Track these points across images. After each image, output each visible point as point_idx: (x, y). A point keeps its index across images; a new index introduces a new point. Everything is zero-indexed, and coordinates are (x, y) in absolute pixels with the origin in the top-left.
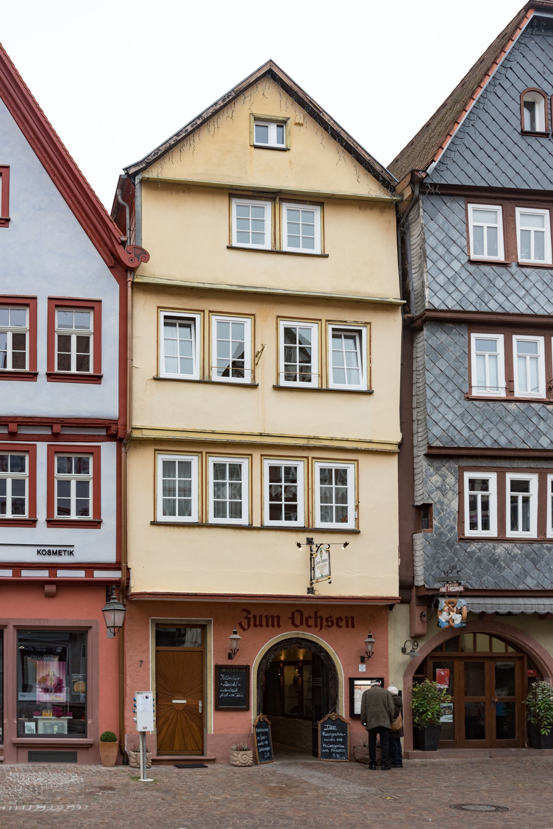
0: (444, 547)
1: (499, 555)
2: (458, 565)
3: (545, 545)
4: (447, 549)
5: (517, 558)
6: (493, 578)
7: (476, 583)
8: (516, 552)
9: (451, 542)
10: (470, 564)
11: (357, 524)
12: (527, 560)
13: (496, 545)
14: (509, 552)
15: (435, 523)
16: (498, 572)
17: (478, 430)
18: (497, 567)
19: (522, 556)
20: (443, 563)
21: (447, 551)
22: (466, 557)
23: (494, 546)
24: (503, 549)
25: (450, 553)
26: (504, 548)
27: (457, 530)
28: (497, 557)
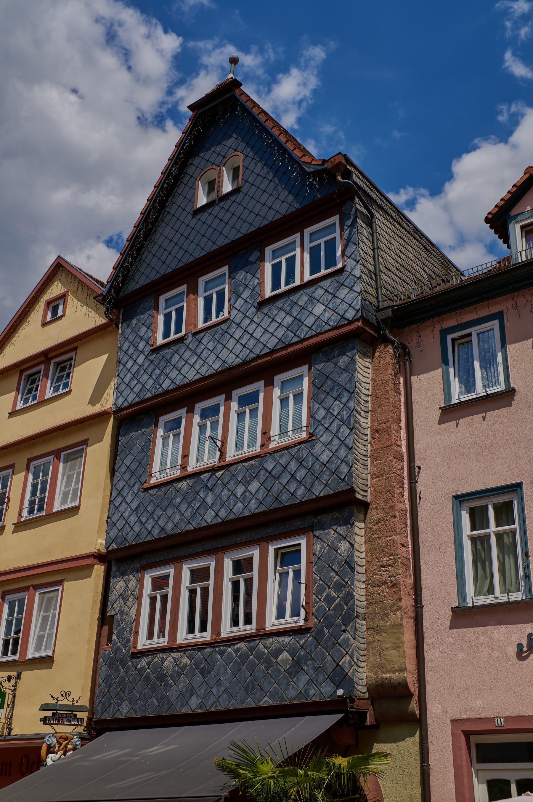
0: (118, 666)
1: (166, 668)
2: (128, 686)
3: (217, 649)
4: (120, 667)
5: (186, 670)
6: (157, 700)
7: (140, 708)
8: (185, 663)
9: (124, 659)
10: (138, 684)
11: (54, 651)
12: (197, 671)
13: (165, 655)
14: (178, 663)
15: (114, 637)
16: (164, 692)
17: (148, 522)
18: (164, 685)
19: (192, 667)
20: (114, 686)
21: (120, 671)
22: (136, 676)
23: (163, 658)
24: (172, 660)
25: (122, 673)
26: (173, 659)
27: (132, 643)
28: (165, 672)
